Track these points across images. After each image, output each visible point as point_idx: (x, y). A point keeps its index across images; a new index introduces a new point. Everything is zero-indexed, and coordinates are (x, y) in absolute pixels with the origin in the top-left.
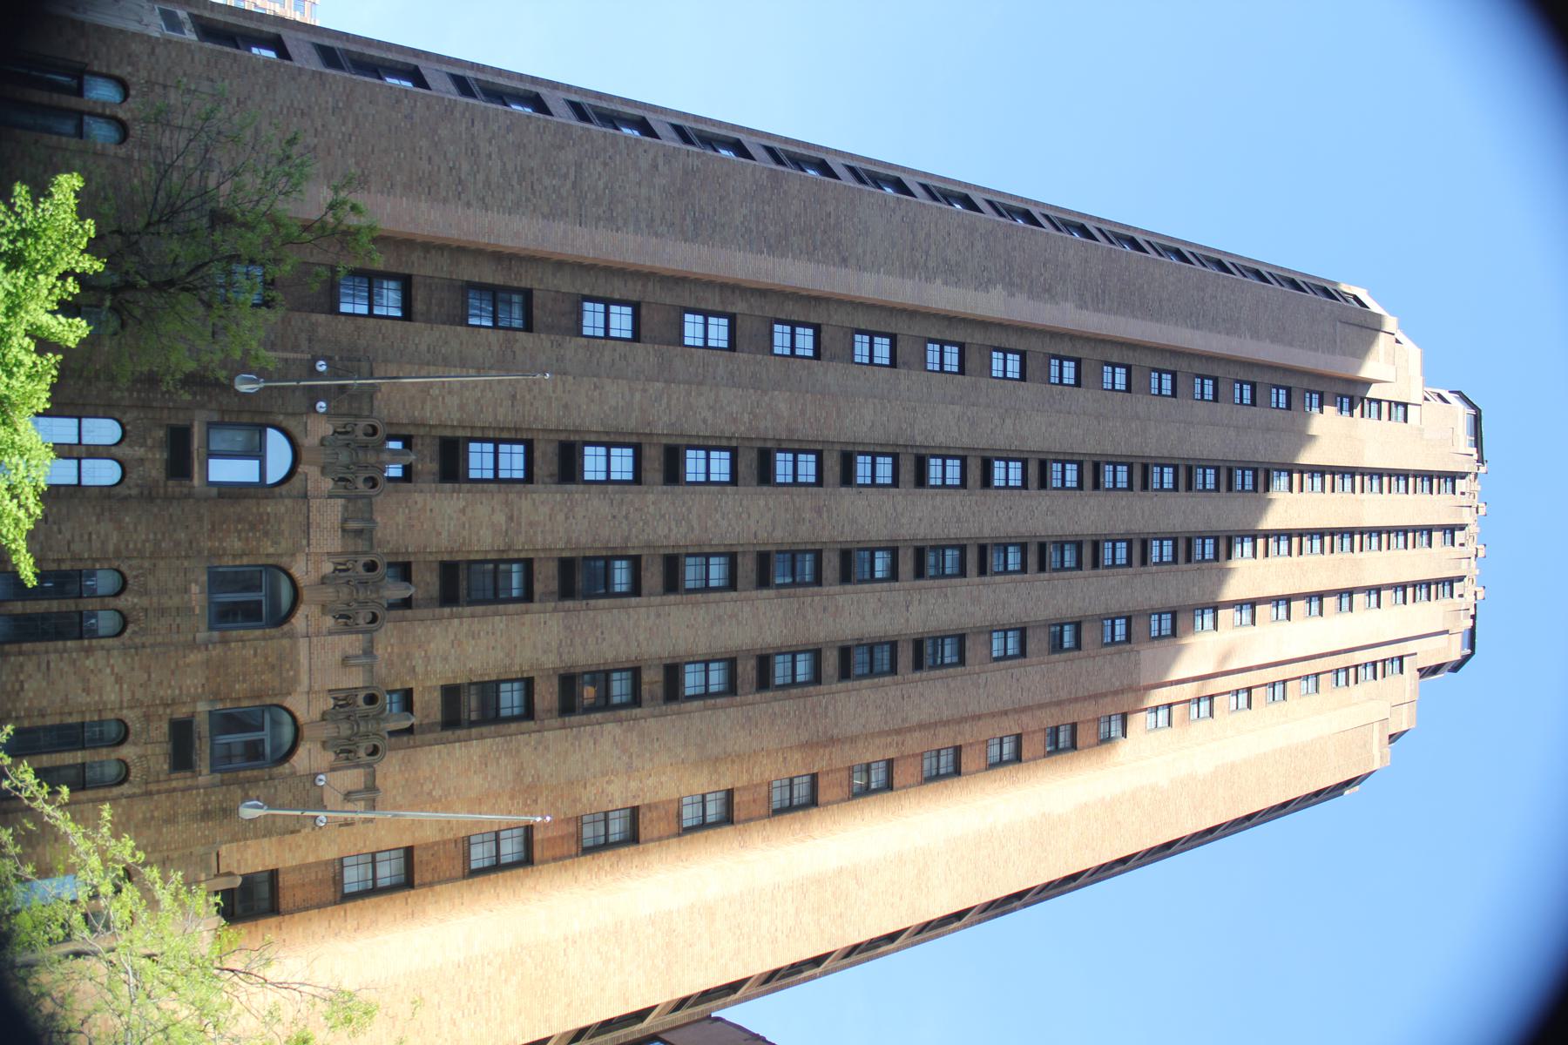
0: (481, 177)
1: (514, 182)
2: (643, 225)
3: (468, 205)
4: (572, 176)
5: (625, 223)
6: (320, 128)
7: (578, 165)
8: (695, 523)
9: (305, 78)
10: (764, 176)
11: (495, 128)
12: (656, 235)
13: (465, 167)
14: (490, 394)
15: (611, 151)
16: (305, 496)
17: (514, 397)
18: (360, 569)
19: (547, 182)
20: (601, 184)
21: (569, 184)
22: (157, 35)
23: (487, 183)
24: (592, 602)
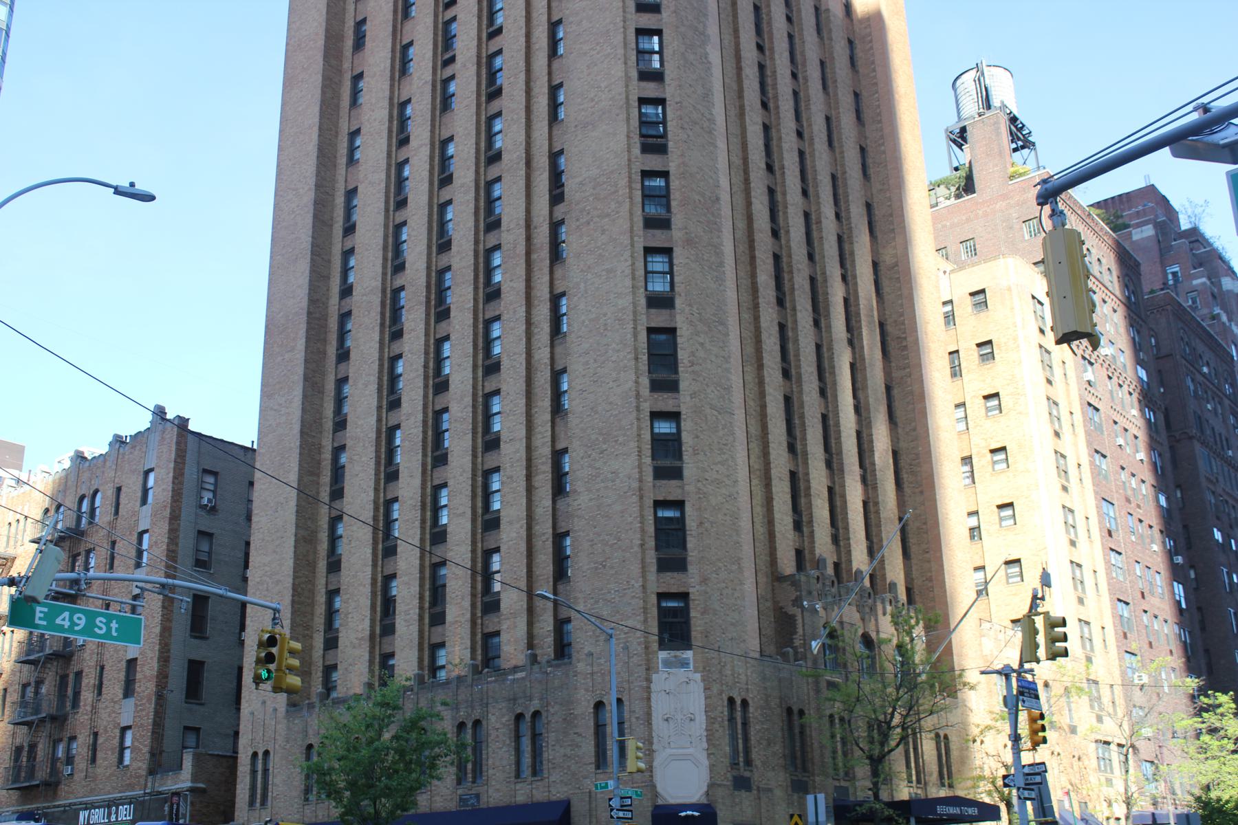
1: (725, 457)
2: (728, 366)
3: (737, 493)
4: (716, 413)
5: (728, 379)
6: (724, 585)
9: (708, 590)
10: (693, 252)
11: (706, 464)
12: (729, 357)
13: (724, 491)
14: (780, 495)
15: (701, 379)
17: (780, 478)
19: (721, 433)
22: (698, 676)
24: (834, 451)
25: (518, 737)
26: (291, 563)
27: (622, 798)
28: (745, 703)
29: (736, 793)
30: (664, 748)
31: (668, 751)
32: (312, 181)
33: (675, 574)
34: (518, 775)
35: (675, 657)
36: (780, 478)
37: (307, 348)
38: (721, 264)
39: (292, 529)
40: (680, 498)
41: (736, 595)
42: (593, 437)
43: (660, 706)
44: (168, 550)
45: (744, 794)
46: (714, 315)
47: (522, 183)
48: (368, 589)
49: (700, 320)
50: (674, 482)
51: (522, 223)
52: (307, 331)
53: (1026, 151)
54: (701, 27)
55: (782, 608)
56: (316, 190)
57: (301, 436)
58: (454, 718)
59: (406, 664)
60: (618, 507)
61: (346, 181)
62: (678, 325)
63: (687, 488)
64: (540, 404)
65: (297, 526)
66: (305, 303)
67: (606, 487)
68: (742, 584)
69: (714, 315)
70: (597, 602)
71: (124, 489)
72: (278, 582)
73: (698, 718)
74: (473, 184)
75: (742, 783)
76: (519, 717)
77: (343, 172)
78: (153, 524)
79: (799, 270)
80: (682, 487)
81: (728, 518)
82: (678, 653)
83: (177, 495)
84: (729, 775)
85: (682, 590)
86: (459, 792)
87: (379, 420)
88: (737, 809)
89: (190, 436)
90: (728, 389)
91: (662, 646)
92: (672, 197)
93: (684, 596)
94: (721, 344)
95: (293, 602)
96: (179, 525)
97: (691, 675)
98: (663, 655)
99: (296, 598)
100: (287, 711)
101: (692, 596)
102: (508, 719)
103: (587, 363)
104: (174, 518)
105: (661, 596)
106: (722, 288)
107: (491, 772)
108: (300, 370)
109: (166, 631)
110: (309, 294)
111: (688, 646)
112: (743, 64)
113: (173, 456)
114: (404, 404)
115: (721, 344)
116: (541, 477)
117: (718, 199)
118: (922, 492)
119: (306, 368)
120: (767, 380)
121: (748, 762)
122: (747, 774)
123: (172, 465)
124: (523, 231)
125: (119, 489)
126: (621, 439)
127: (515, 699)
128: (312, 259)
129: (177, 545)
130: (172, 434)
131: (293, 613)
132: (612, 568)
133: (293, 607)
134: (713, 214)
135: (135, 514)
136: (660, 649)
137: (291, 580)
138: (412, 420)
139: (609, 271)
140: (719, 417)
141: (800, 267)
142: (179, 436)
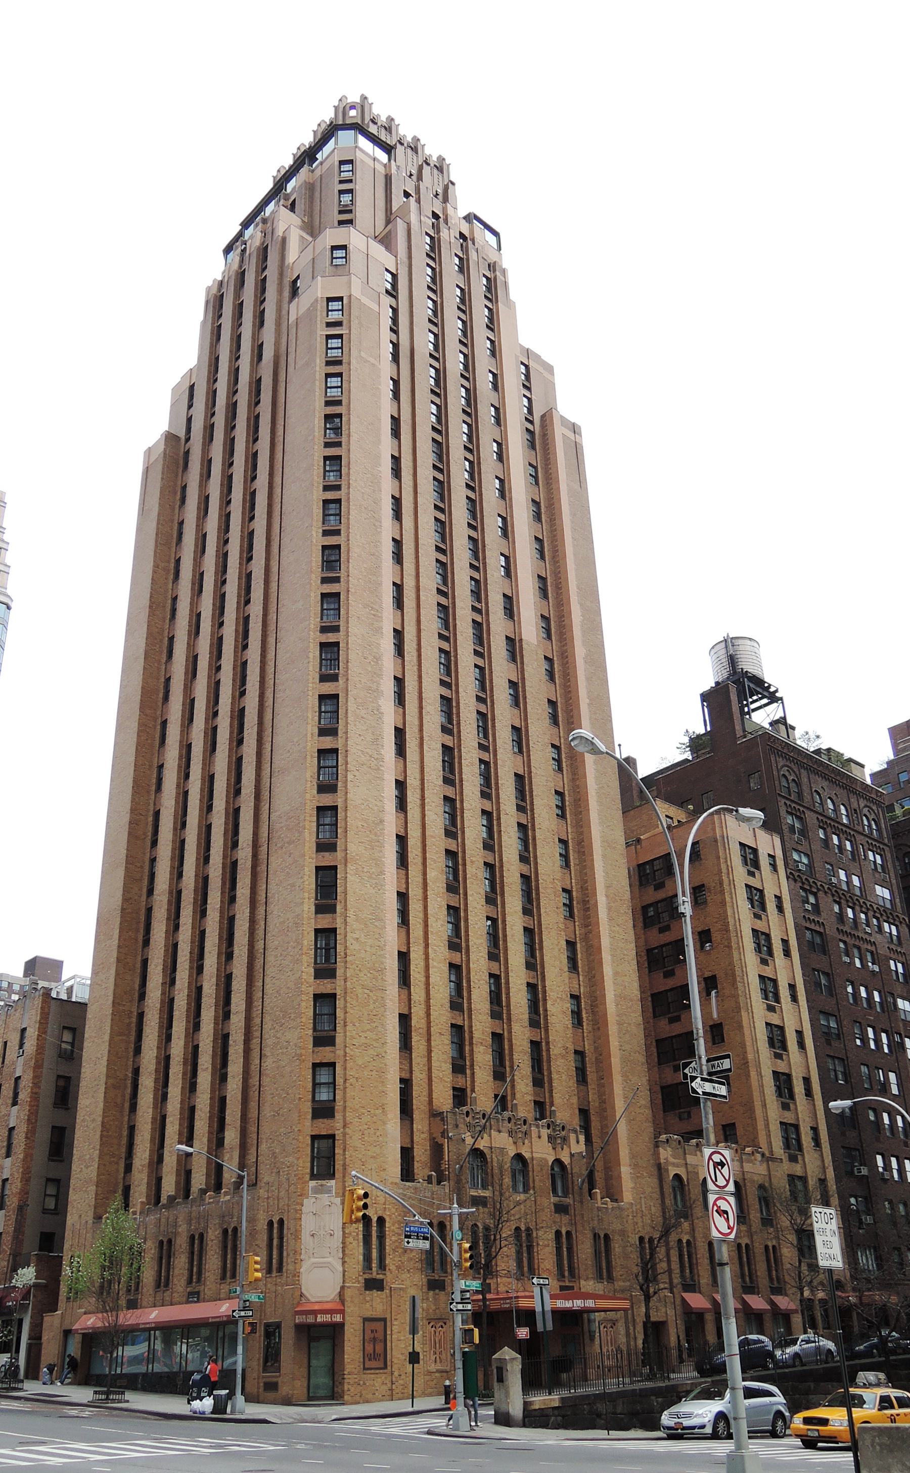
0: (375, 1044)
1: (375, 1025)
2: (382, 952)
3: (386, 1052)
4: (367, 991)
7: (363, 987)
8: (480, 941)
12: (385, 945)
13: (371, 1052)
15: (354, 966)
16: (491, 1148)
17: (440, 1033)
18: (510, 1125)
19: (371, 1007)
20: (369, 975)
21: (371, 994)
22: (338, 1201)
23: (376, 1040)
25: (225, 1248)
26: (101, 1105)
27: (245, 1301)
28: (381, 1221)
29: (367, 1292)
30: (309, 1257)
31: (313, 1260)
32: (128, 807)
33: (325, 1120)
34: (223, 1277)
35: (322, 1185)
36: (440, 1033)
37: (120, 937)
38: (382, 873)
39: (103, 1079)
40: (332, 1060)
41: (378, 1133)
42: (277, 1013)
43: (308, 1224)
44: (32, 1093)
45: (375, 1293)
46: (372, 914)
47: (252, 812)
48: (149, 1126)
49: (357, 920)
50: (328, 1049)
51: (251, 843)
52: (121, 924)
53: (775, 705)
54: (374, 686)
55: (434, 1138)
56: (131, 813)
57: (113, 1006)
58: (188, 1231)
59: (169, 1186)
60: (288, 1069)
61: (155, 804)
62: (338, 926)
63: (338, 1052)
64: (257, 984)
65: (108, 1077)
66: (120, 903)
67: (282, 1053)
68: (384, 1123)
69: (372, 914)
70: (273, 1142)
71: (8, 1044)
72: (94, 1120)
73: (335, 1236)
74: (224, 812)
75: (374, 1285)
76: (225, 1232)
77: (153, 797)
78: (24, 1072)
79: (472, 862)
80: (334, 1052)
81: (374, 1073)
82: (324, 1182)
83: (40, 1049)
84: (360, 1278)
85: (330, 1132)
86: (188, 1290)
87: (163, 994)
88: (368, 1305)
89: (53, 1002)
90: (382, 971)
91: (313, 1177)
92: (339, 825)
93: (332, 1137)
94: (377, 936)
95: (102, 1136)
96: (41, 1072)
97: (333, 1199)
98: (312, 1184)
99: (105, 1133)
100: (94, 1223)
101: (337, 1137)
102: (218, 1232)
103: (276, 956)
104: (38, 1066)
105: (314, 1138)
106: (381, 891)
107: (207, 1274)
108: (115, 954)
109: (28, 1156)
110: (124, 894)
111: (332, 1176)
112: (424, 703)
113: (38, 1018)
114: (177, 982)
115: (377, 936)
116: (254, 1041)
117: (382, 821)
118: (599, 1028)
119: (118, 952)
120: (431, 955)
121: (382, 1266)
122: (380, 1277)
123: (37, 1026)
124: (250, 849)
125: (6, 1043)
126: (293, 1016)
127: (224, 1217)
128: (126, 867)
129: (39, 1087)
130: (38, 1002)
131: (101, 1145)
132: (283, 1115)
133: (101, 1139)
134: (376, 835)
135: (14, 1063)
136: (311, 1180)
137: (100, 1119)
138: (181, 995)
139: (293, 885)
140: (371, 994)
141: (474, 859)
142: (44, 1002)
